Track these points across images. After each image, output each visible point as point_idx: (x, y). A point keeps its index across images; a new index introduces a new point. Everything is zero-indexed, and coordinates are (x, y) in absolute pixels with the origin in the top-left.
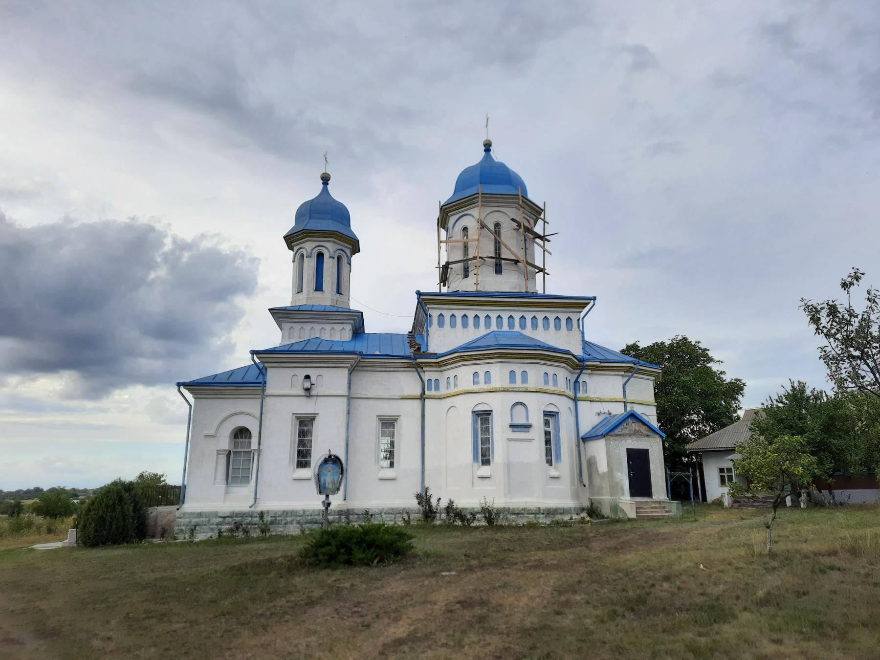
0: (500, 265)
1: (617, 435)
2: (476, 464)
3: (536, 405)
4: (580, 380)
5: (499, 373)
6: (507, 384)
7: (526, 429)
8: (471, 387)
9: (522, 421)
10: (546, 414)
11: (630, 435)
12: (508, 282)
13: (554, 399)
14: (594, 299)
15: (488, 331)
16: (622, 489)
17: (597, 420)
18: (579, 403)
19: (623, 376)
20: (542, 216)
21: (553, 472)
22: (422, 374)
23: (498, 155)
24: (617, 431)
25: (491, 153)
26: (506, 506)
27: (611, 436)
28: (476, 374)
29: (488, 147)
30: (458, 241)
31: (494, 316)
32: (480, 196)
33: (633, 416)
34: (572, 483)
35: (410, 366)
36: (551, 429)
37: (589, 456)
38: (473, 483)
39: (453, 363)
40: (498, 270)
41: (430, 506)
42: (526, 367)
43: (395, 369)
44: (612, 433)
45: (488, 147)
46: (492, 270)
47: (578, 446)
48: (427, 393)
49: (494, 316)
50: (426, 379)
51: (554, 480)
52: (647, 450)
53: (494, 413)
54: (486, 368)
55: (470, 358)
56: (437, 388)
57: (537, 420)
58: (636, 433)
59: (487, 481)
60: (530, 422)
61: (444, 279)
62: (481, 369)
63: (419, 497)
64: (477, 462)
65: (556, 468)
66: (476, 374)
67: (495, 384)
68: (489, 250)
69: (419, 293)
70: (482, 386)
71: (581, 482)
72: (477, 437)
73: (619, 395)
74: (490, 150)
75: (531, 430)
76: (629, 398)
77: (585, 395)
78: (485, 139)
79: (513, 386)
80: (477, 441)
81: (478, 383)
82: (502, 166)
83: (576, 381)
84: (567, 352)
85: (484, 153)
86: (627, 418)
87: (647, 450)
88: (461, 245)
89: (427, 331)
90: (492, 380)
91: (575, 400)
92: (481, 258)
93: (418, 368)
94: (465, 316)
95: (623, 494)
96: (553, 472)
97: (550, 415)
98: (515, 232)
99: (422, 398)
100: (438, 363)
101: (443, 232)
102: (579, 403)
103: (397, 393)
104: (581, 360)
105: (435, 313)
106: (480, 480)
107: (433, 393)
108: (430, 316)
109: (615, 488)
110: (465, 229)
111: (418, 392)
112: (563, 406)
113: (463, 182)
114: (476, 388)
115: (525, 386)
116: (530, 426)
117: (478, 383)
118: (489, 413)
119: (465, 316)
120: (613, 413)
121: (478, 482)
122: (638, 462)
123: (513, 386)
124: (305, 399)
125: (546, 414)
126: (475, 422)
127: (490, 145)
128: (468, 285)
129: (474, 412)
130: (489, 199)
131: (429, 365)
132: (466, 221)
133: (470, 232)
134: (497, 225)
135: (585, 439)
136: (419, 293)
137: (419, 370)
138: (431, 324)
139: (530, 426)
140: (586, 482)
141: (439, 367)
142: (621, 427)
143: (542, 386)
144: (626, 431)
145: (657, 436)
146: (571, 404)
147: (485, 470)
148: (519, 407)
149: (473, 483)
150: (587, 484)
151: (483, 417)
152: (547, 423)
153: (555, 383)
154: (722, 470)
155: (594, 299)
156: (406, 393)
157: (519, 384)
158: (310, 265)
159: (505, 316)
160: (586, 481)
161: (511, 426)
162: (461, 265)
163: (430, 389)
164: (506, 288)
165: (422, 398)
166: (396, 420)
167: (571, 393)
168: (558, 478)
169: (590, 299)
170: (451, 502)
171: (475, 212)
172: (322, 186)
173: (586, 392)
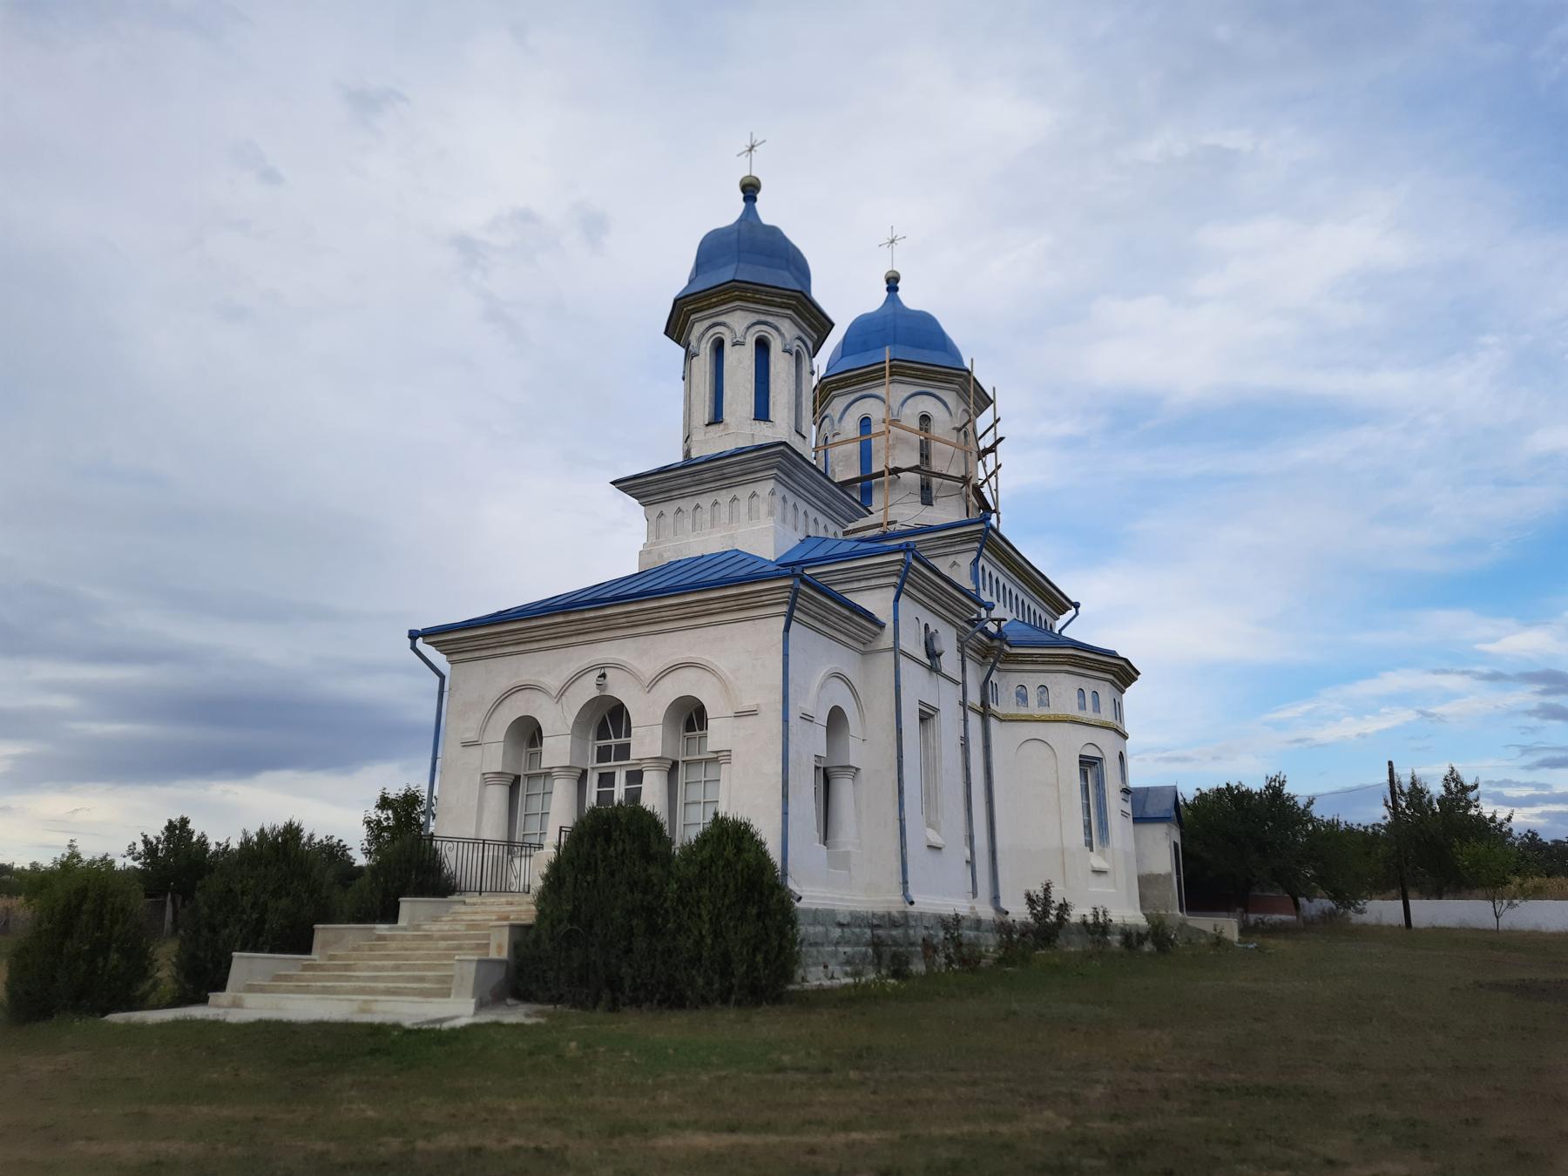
14: (1077, 606)
29: (892, 283)
30: (911, 431)
45: (892, 283)
59: (1103, 877)
74: (897, 289)
88: (916, 439)
106: (1094, 876)
110: (925, 419)
124: (923, 671)
127: (897, 279)
133: (937, 429)
155: (1077, 606)
158: (740, 363)
162: (914, 478)
172: (743, 205)
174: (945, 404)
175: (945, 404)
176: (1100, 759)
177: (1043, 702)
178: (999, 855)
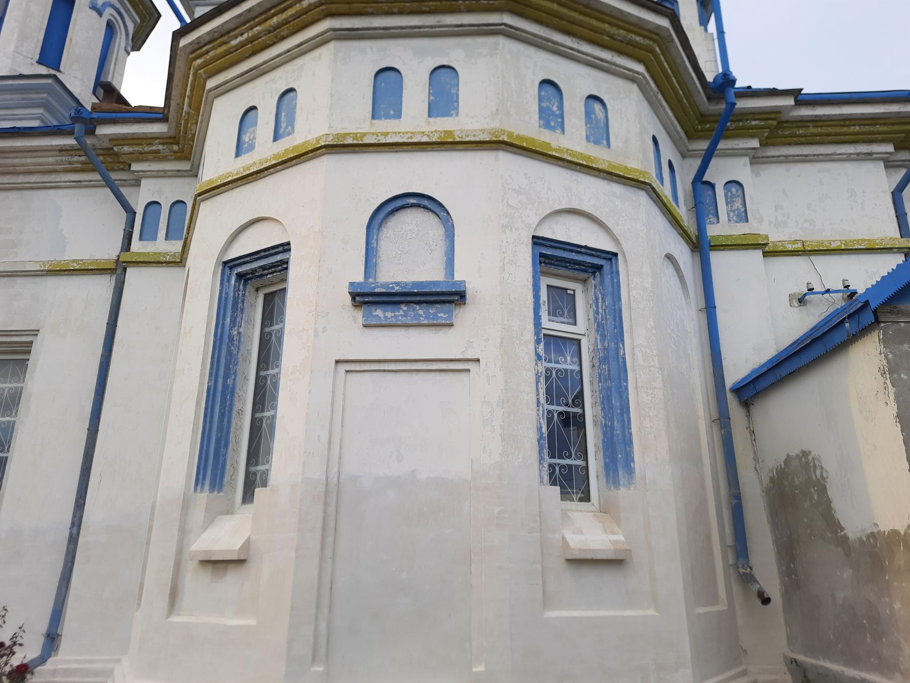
7: (439, 313)
19: (889, 164)
34: (700, 587)
36: (581, 326)
37: (774, 457)
42: (453, 52)
47: (723, 421)
50: (140, 200)
51: (592, 578)
57: (497, 273)
64: (217, 483)
65: (606, 510)
71: (747, 578)
75: (463, 316)
96: (586, 530)
97: (568, 265)
116: (452, 297)
121: (195, 582)
135: (756, 388)
139: (452, 297)
140: (769, 577)
143: (527, 125)
149: (174, 595)
150: (774, 590)
153: (600, 132)
160: (769, 577)
161: (365, 298)
163: (148, 234)
168: (614, 563)
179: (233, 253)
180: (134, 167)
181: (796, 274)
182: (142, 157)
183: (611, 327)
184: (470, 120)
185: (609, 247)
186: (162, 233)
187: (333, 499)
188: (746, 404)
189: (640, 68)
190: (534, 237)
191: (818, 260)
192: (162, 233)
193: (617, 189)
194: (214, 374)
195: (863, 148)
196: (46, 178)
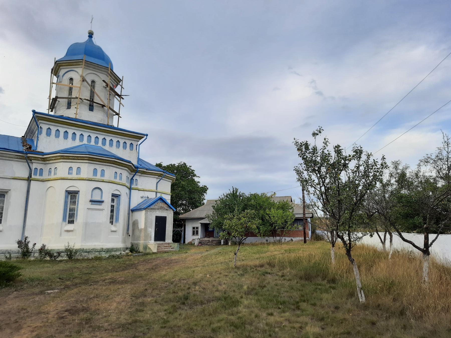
0: (93, 106)
1: (152, 209)
2: (64, 223)
3: (108, 191)
4: (134, 178)
5: (86, 169)
6: (91, 176)
7: (100, 203)
8: (66, 175)
9: (98, 198)
10: (113, 195)
11: (158, 209)
12: (96, 116)
13: (119, 187)
14: (147, 135)
15: (81, 143)
16: (151, 237)
17: (141, 200)
18: (132, 191)
19: (157, 178)
20: (121, 83)
21: (113, 228)
22: (30, 164)
23: (97, 41)
24: (152, 207)
25: (93, 39)
26: (82, 248)
27: (149, 209)
28: (71, 168)
29: (91, 35)
30: (66, 85)
31: (86, 135)
32: (84, 62)
33: (161, 199)
34: (123, 235)
35: (22, 158)
37: (134, 220)
38: (61, 235)
39: (55, 160)
40: (91, 108)
41: (28, 249)
42: (105, 168)
43: (10, 158)
44: (149, 208)
45: (91, 35)
46: (87, 108)
47: (129, 214)
48: (33, 176)
49: (86, 135)
51: (113, 233)
52: (166, 217)
53: (80, 193)
54: (78, 165)
55: (68, 158)
56: (41, 174)
57: (107, 198)
58: (161, 208)
59: (71, 233)
60: (103, 199)
61: (52, 106)
62: (75, 166)
63: (19, 243)
64: (65, 221)
65: (114, 226)
66: (71, 168)
67: (83, 175)
68: (87, 95)
69: (34, 112)
70: (74, 175)
71: (128, 233)
72: (67, 207)
73: (154, 189)
74: (92, 37)
75: (103, 204)
76: (159, 190)
77: (136, 187)
78: (90, 29)
79: (95, 177)
80: (67, 209)
81: (71, 174)
82: (99, 49)
83: (132, 179)
84: (129, 162)
85: (88, 38)
86: (158, 200)
87: (166, 217)
89: (38, 137)
90: (81, 173)
91: (130, 189)
92: (81, 99)
93: (29, 160)
94: (66, 132)
95: (151, 240)
96: (113, 228)
97: (115, 196)
98: (104, 88)
99: (29, 179)
100: (44, 158)
101: (55, 79)
102: (132, 191)
103: (10, 175)
104: (137, 168)
105: (45, 127)
106: (66, 233)
107: (38, 177)
108: (41, 128)
109: (147, 236)
110: (71, 79)
111: (26, 176)
112: (124, 191)
113: (73, 50)
114: (70, 176)
115: (103, 178)
116: (103, 202)
117: (71, 174)
118: (77, 192)
119: (66, 132)
120: (150, 197)
121: (64, 234)
122: (160, 223)
123: (95, 177)
125: (113, 195)
126: (66, 197)
127: (92, 34)
128: (71, 113)
129: (66, 191)
130: (88, 65)
131: (36, 159)
132: (71, 75)
133: (74, 82)
134: (93, 82)
135: (133, 211)
136: (34, 112)
137: (29, 161)
138: (41, 133)
139: (103, 202)
140: (130, 233)
141: (44, 161)
142: (155, 204)
143: (113, 179)
144: (156, 207)
145: (171, 210)
146: (128, 191)
147: (70, 227)
148: (97, 191)
150: (131, 235)
151: (72, 195)
152: (113, 200)
153: (121, 178)
154: (194, 228)
155: (147, 135)
156: (17, 175)
157: (99, 177)
159: (93, 136)
160: (130, 233)
161: (91, 201)
162: (66, 100)
163: (36, 174)
164: (96, 121)
165: (29, 179)
166: (7, 192)
167: (128, 185)
169: (144, 135)
170: (44, 246)
171: (80, 70)
173: (137, 185)
174: (78, 72)
175: (78, 72)
176: (79, 191)
177: (55, 174)
178: (27, 227)
179: (68, 190)
180: (33, 161)
181: (142, 194)
182: (35, 160)
183: (119, 204)
184: (106, 178)
185: (120, 194)
186: (38, 175)
187: (86, 225)
188: (132, 212)
189: (127, 169)
190: (112, 194)
191: (145, 192)
192: (38, 175)
193: (122, 186)
194: (65, 207)
195: (154, 176)
196: (10, 159)
